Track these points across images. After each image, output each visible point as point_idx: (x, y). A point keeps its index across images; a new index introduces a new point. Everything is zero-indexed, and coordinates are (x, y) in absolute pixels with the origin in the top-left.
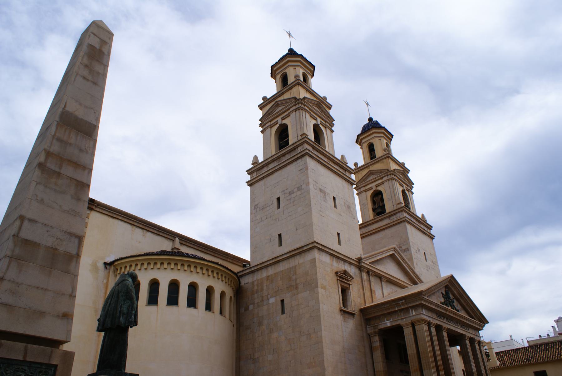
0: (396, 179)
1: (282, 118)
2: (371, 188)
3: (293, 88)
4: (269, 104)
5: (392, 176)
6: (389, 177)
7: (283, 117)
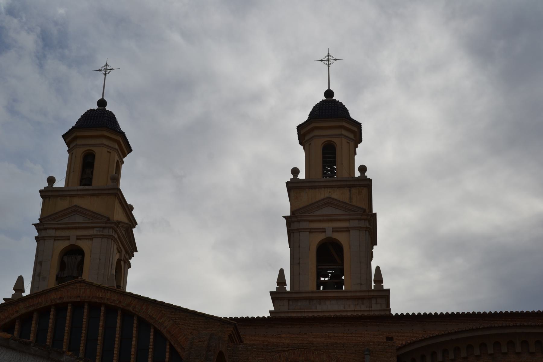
0: (116, 239)
1: (333, 228)
2: (68, 238)
5: (111, 230)
6: (106, 232)
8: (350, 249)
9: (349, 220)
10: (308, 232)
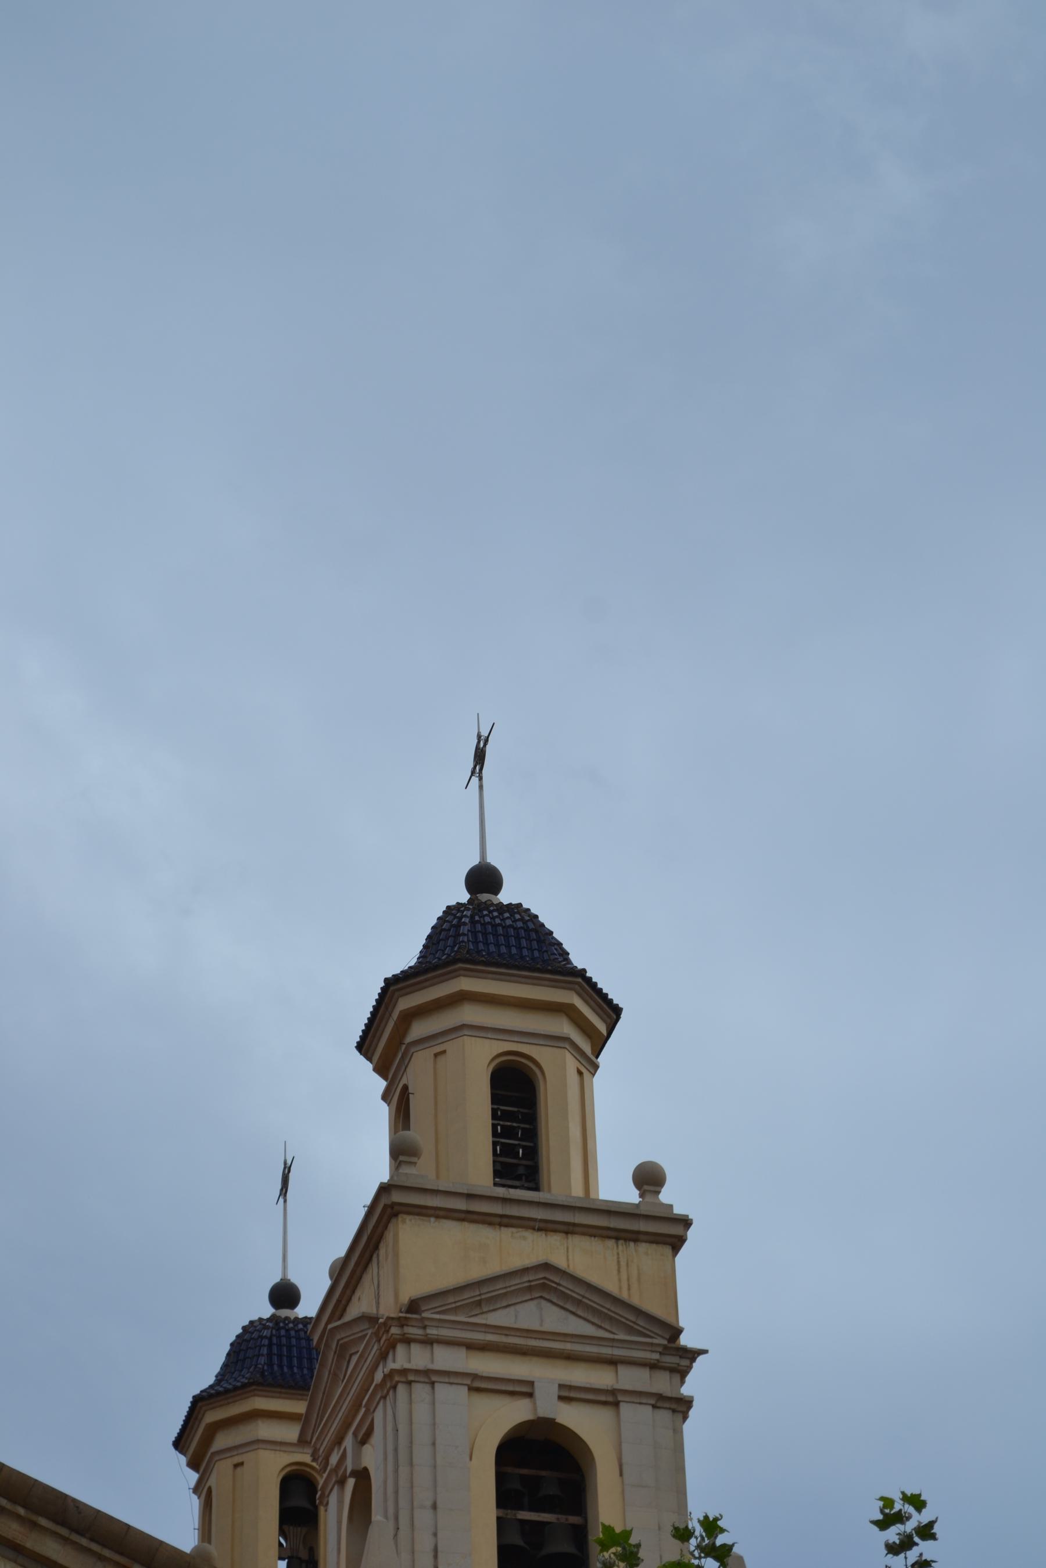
3: (636, 1241)
4: (463, 1220)
7: (570, 1388)
8: (621, 1475)
9: (613, 1362)
10: (466, 1388)
